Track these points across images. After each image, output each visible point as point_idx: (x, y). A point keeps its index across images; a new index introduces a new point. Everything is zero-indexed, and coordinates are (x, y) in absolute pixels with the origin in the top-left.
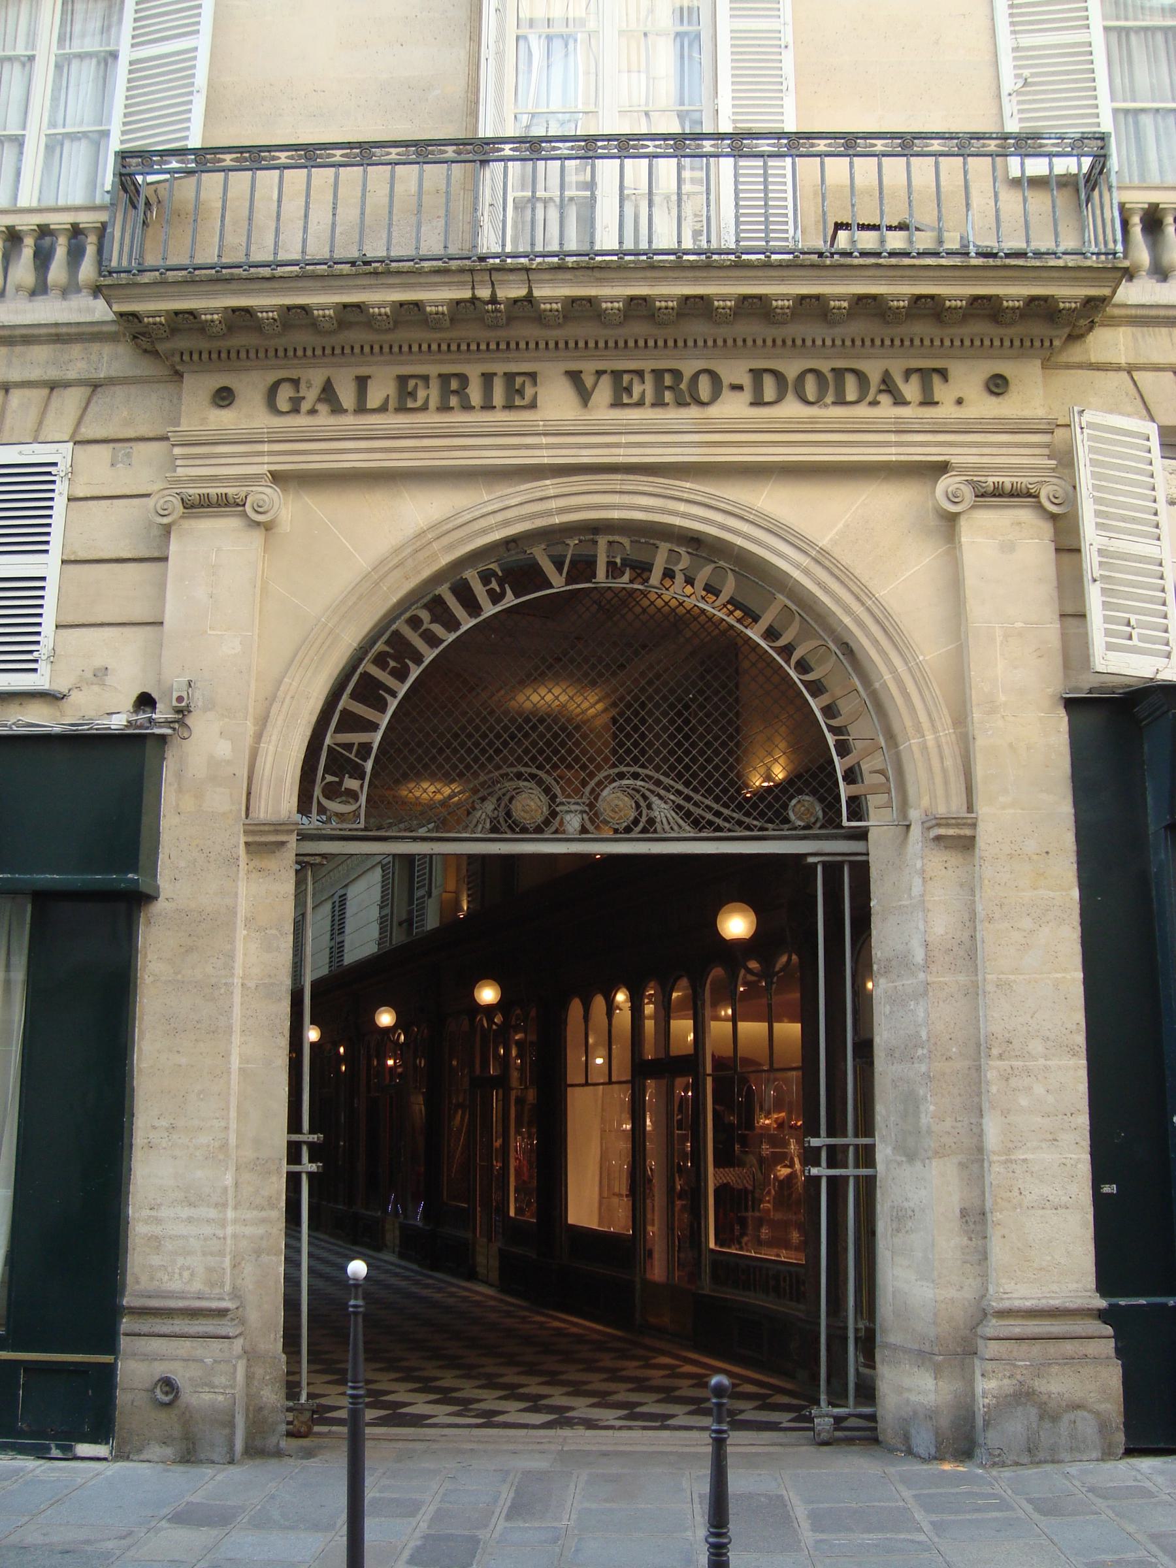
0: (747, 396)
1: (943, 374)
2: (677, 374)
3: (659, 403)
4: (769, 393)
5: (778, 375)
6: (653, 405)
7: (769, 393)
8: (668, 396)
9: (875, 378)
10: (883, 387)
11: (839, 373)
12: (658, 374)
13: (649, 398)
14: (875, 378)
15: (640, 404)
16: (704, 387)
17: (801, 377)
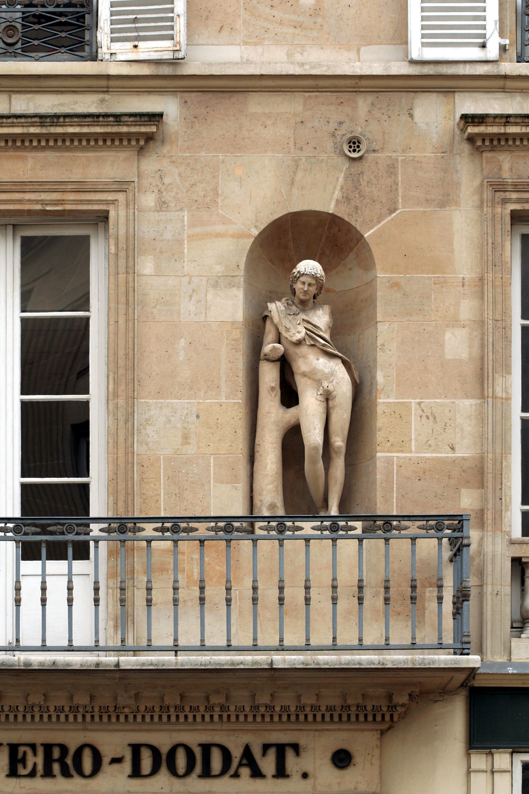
0: (127, 767)
1: (296, 748)
2: (64, 749)
3: (48, 773)
4: (146, 764)
5: (155, 751)
6: (44, 776)
7: (146, 764)
8: (56, 767)
9: (237, 753)
10: (245, 761)
11: (206, 748)
12: (48, 748)
13: (40, 768)
14: (237, 753)
15: (32, 774)
16: (87, 765)
17: (172, 753)
